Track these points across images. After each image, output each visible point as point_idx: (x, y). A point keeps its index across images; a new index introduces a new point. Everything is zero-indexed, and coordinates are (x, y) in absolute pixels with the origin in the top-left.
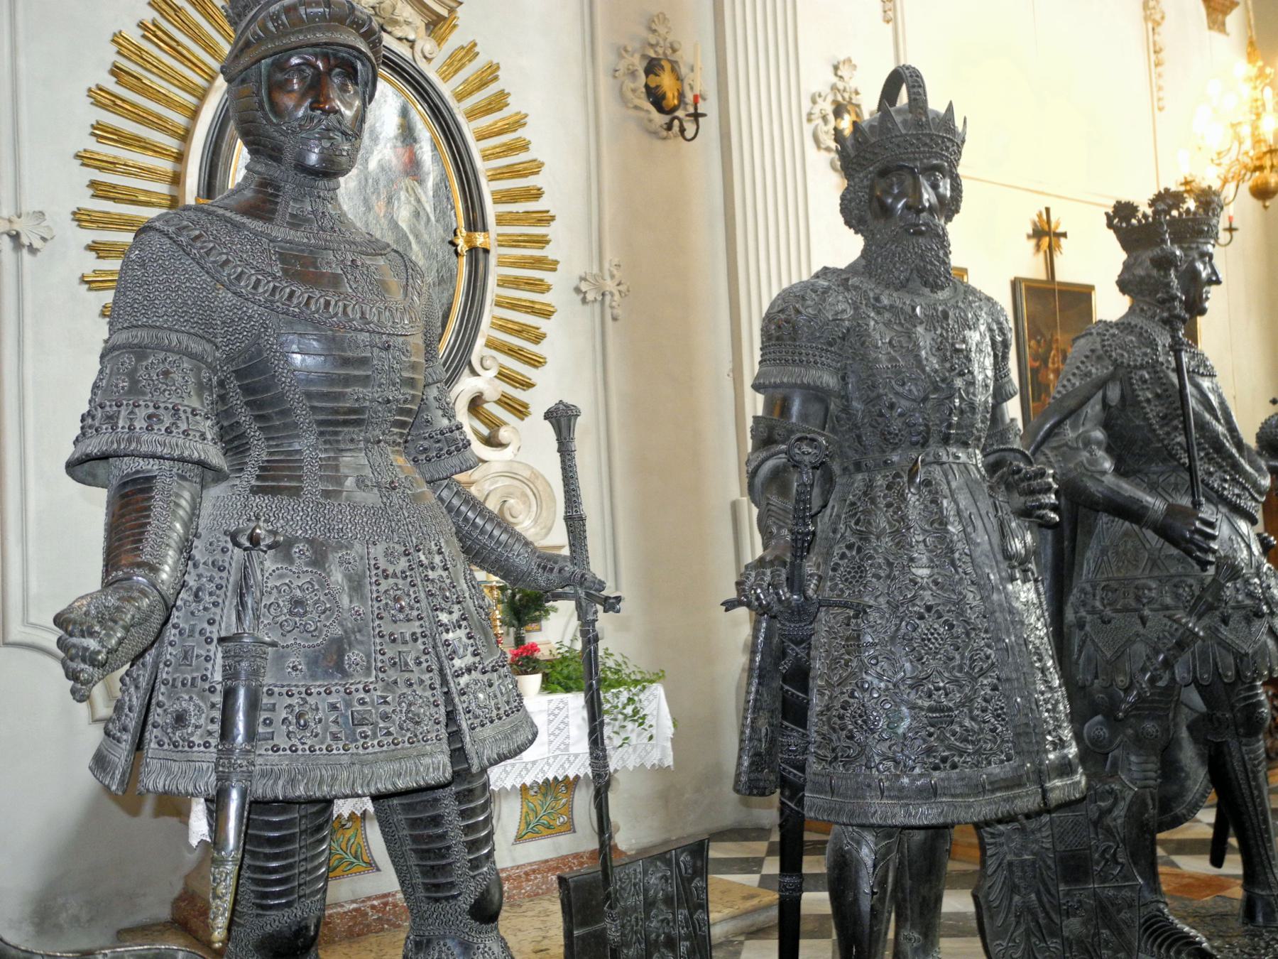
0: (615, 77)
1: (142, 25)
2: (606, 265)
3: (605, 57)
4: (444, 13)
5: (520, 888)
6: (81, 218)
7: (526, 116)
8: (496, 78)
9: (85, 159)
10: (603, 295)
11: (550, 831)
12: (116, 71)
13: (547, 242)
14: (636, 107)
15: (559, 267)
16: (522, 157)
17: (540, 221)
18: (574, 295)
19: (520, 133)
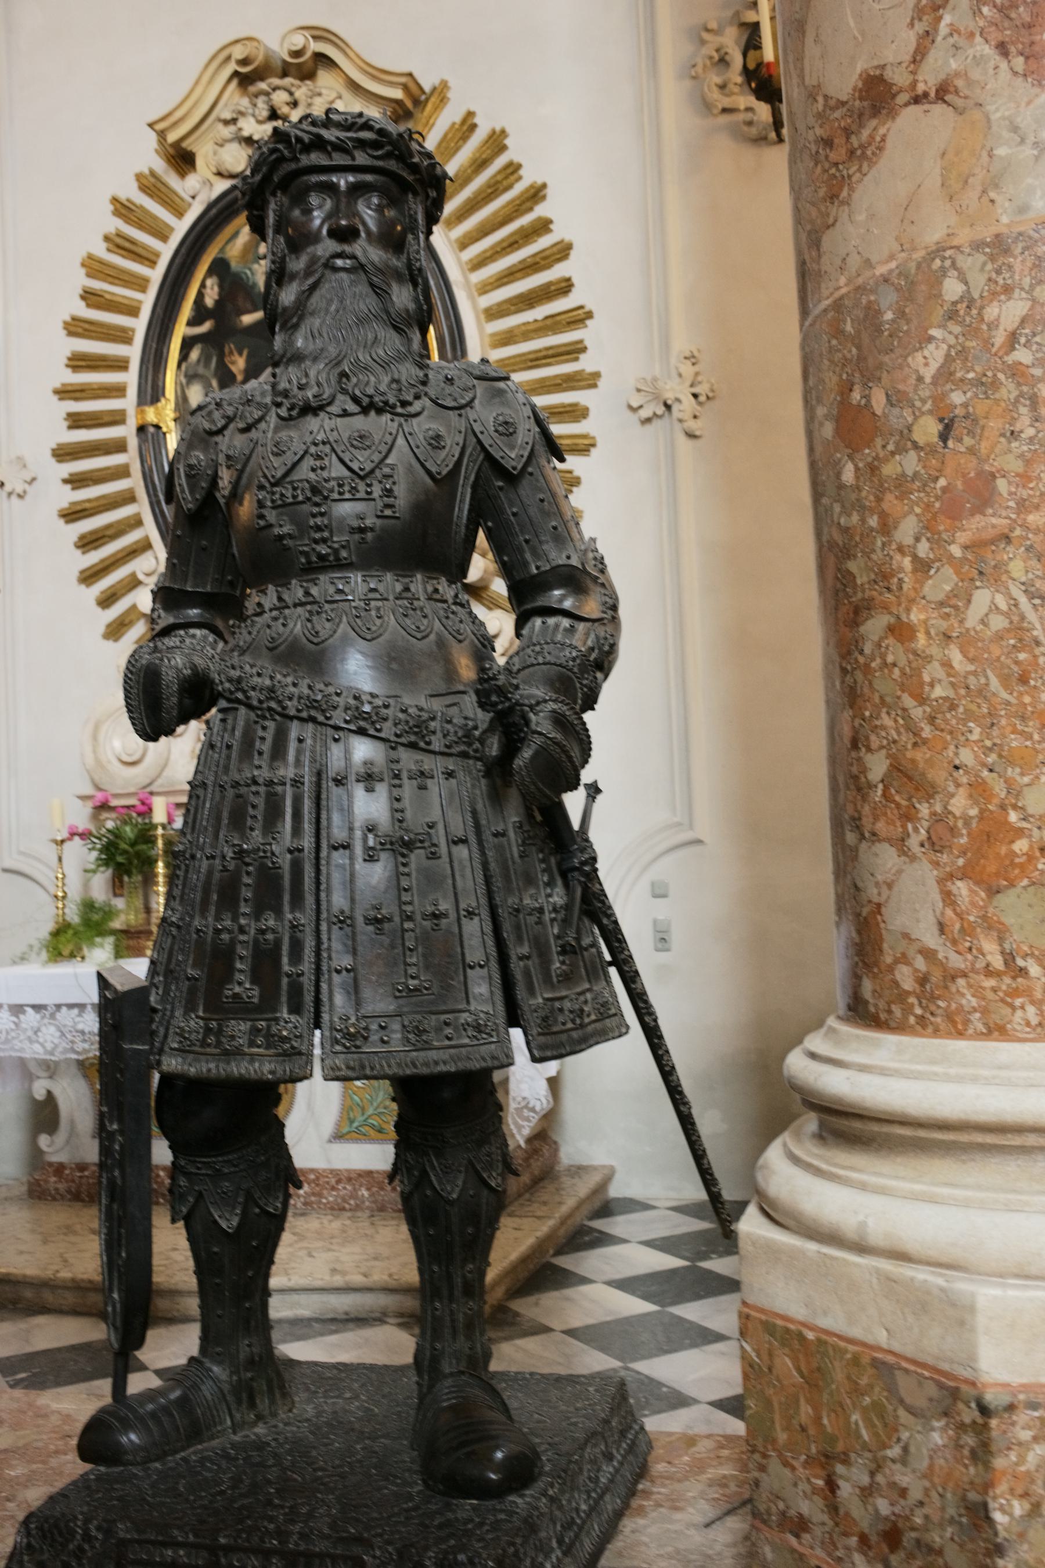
0: (694, 78)
1: (107, 238)
2: (673, 361)
3: (672, 50)
4: (398, 94)
5: (320, 1195)
6: (63, 453)
7: (544, 186)
8: (503, 148)
9: (64, 393)
10: (668, 407)
11: (380, 1136)
12: (89, 297)
13: (584, 350)
14: (725, 110)
15: (601, 383)
16: (544, 242)
17: (569, 323)
18: (629, 414)
19: (541, 210)
